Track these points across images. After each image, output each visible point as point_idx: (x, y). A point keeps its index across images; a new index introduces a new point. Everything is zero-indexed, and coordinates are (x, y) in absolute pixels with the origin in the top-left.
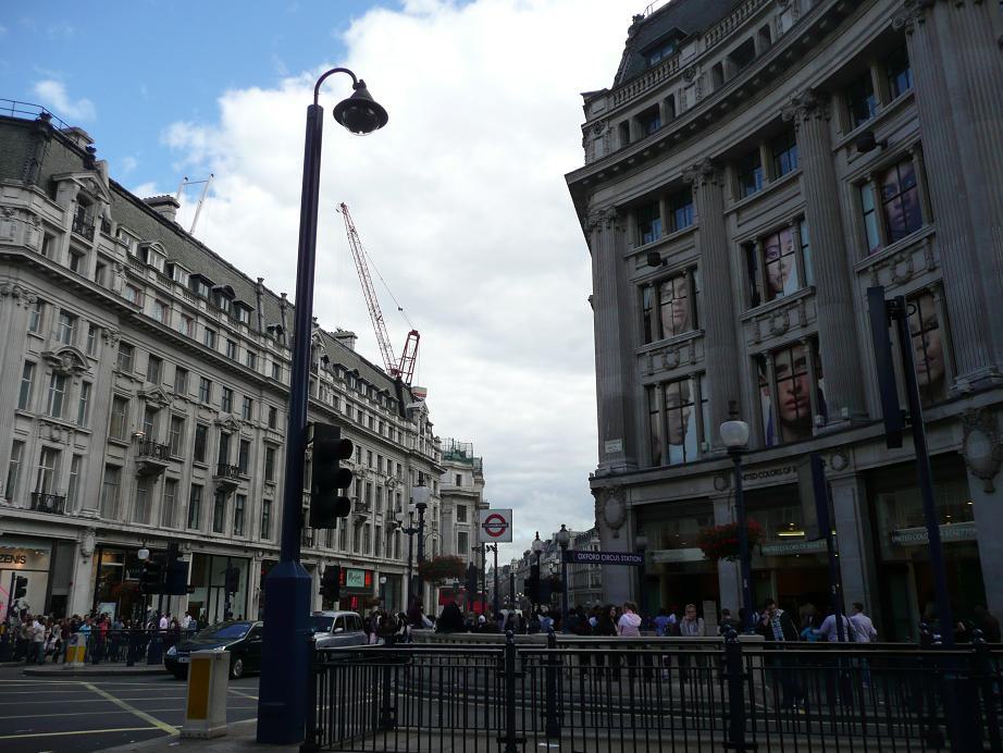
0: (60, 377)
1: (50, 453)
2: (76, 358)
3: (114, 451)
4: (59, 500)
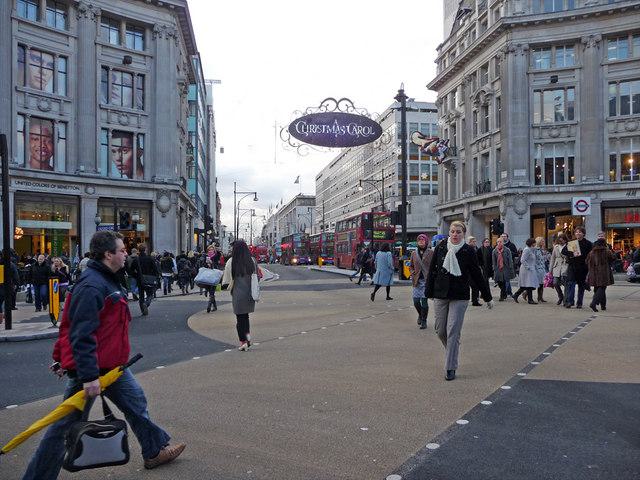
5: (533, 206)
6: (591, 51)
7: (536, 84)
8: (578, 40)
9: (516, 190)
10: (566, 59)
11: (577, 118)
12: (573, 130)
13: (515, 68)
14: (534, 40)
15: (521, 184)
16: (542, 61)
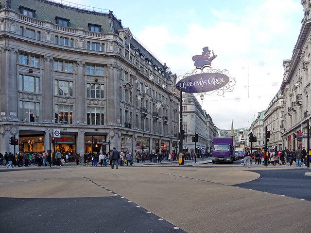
0: (126, 90)
1: (126, 111)
2: (130, 85)
3: (137, 111)
4: (130, 125)
6: (48, 63)
7: (20, 70)
8: (43, 56)
9: (12, 123)
10: (35, 62)
11: (74, 96)
13: (10, 60)
14: (21, 49)
16: (23, 60)
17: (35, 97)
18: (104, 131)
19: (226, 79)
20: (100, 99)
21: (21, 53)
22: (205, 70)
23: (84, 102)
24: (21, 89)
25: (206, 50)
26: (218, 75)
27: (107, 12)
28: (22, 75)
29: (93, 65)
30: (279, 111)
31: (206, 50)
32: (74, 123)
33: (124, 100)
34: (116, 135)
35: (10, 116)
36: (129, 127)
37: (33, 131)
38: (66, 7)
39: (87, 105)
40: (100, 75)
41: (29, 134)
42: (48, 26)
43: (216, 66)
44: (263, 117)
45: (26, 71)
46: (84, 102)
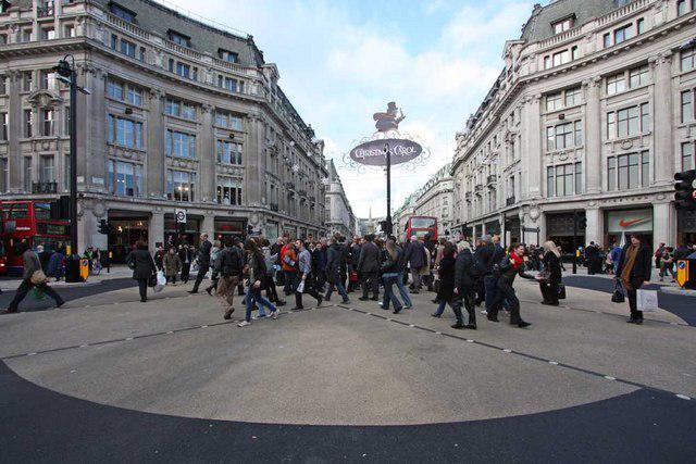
1: (272, 187)
5: (110, 211)
12: (142, 157)
14: (113, 72)
15: (100, 191)
16: (115, 90)
17: (134, 155)
18: (243, 215)
19: (418, 149)
20: (237, 165)
21: (112, 78)
22: (391, 134)
23: (213, 168)
24: (111, 142)
25: (392, 106)
26: (408, 143)
27: (245, 36)
28: (113, 116)
29: (227, 112)
30: (441, 196)
31: (392, 106)
32: (196, 200)
33: (269, 169)
34: (261, 222)
35: (92, 184)
36: (276, 211)
37: (118, 210)
38: (184, 18)
39: (217, 174)
40: (236, 128)
41: (120, 215)
42: (156, 41)
43: (404, 131)
44: (414, 203)
45: (121, 111)
46: (213, 168)
